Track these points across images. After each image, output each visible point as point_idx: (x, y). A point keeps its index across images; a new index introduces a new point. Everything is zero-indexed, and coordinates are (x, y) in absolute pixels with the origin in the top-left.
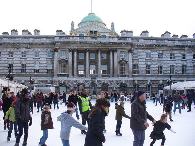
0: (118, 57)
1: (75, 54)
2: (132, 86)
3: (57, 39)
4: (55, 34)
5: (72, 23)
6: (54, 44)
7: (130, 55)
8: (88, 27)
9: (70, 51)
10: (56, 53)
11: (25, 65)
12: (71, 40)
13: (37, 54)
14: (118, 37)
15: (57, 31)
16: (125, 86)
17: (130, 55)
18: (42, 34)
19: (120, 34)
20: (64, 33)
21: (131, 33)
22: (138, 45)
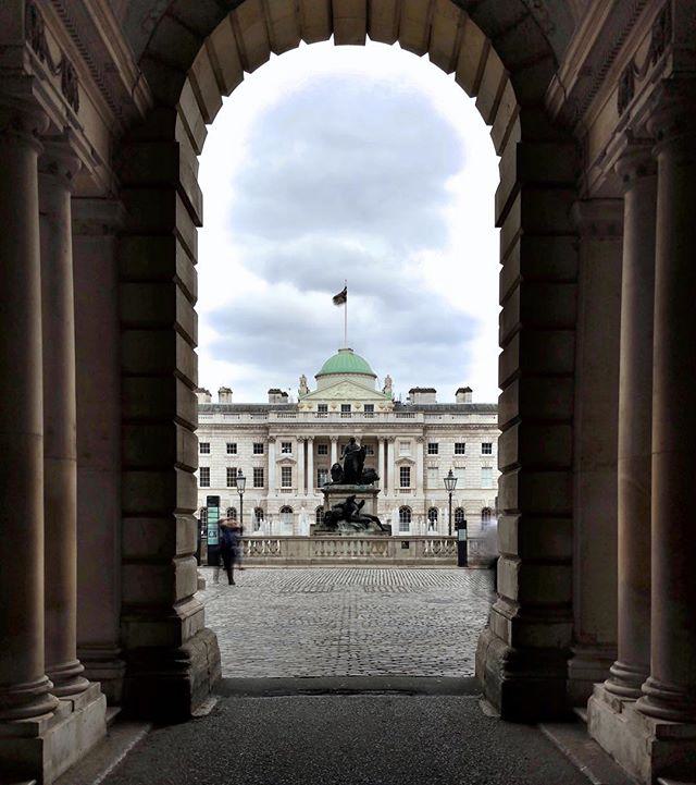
0: (396, 454)
1: (310, 447)
2: (423, 512)
3: (273, 418)
4: (263, 399)
5: (303, 382)
6: (266, 428)
7: (420, 446)
8: (335, 389)
9: (299, 441)
10: (271, 445)
11: (208, 469)
12: (300, 418)
13: (232, 448)
14: (397, 407)
15: (271, 392)
16: (409, 511)
17: (420, 446)
18: (238, 399)
19: (404, 401)
20: (285, 395)
21: (432, 394)
22: (440, 427)
